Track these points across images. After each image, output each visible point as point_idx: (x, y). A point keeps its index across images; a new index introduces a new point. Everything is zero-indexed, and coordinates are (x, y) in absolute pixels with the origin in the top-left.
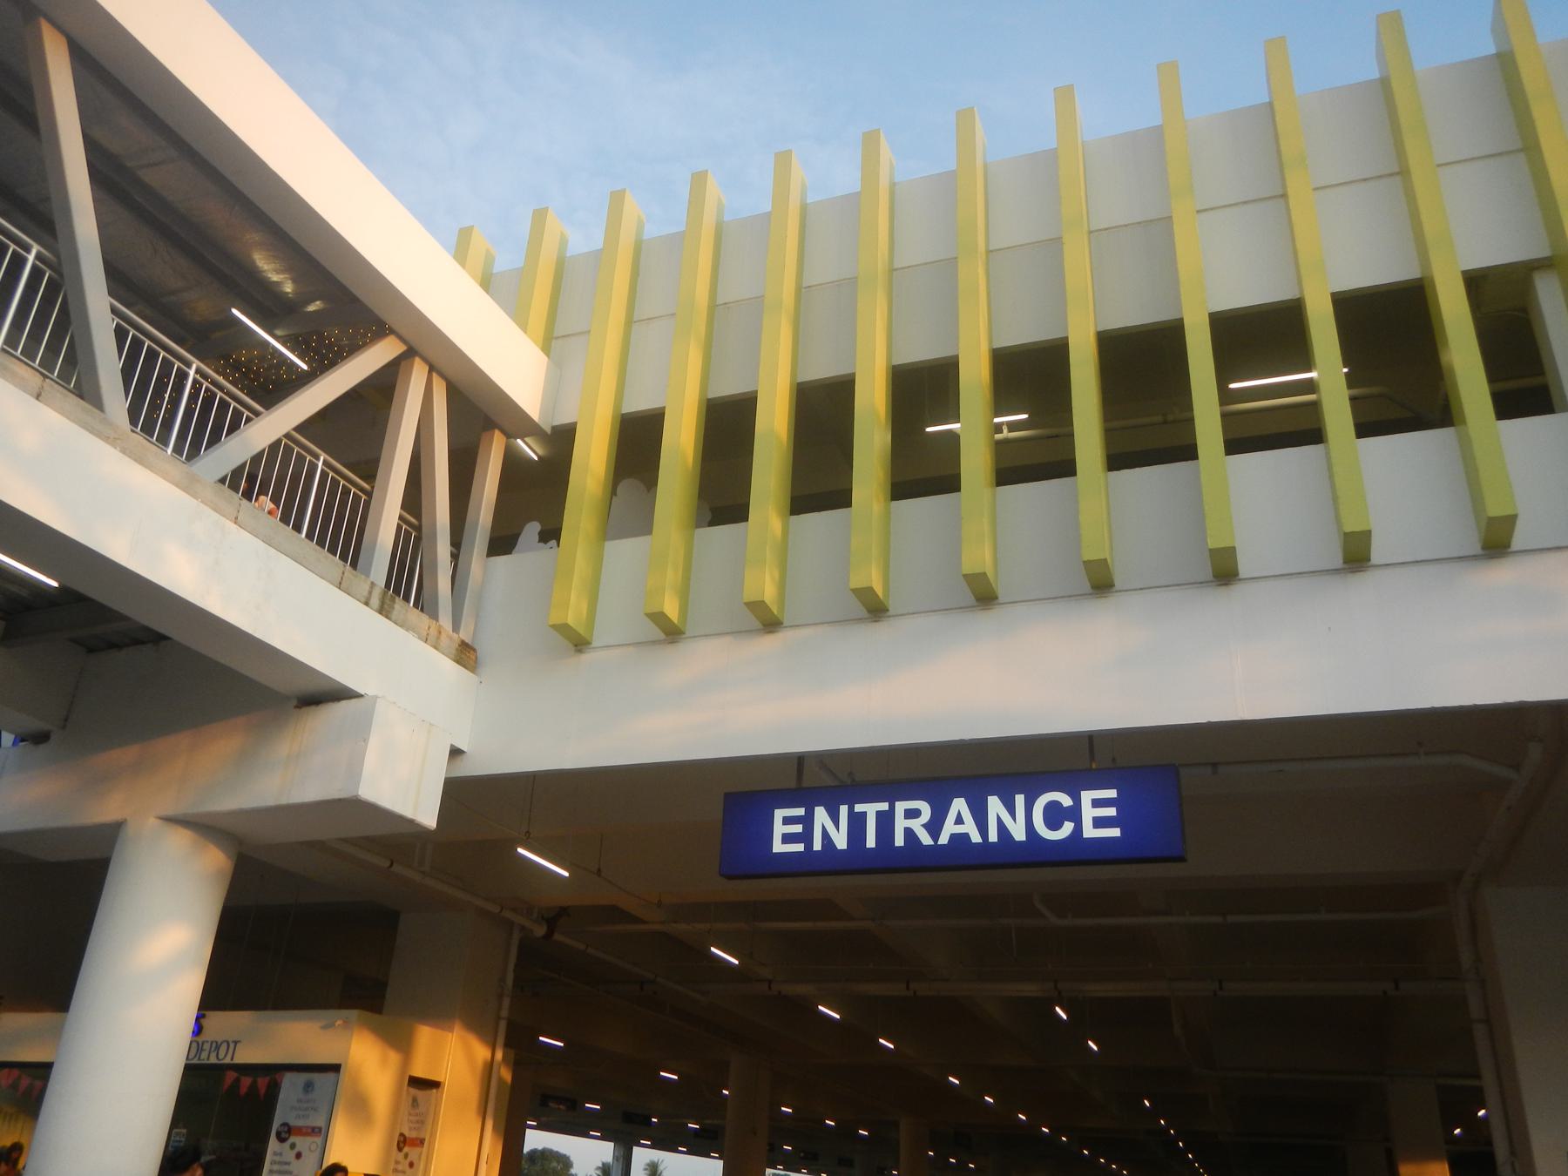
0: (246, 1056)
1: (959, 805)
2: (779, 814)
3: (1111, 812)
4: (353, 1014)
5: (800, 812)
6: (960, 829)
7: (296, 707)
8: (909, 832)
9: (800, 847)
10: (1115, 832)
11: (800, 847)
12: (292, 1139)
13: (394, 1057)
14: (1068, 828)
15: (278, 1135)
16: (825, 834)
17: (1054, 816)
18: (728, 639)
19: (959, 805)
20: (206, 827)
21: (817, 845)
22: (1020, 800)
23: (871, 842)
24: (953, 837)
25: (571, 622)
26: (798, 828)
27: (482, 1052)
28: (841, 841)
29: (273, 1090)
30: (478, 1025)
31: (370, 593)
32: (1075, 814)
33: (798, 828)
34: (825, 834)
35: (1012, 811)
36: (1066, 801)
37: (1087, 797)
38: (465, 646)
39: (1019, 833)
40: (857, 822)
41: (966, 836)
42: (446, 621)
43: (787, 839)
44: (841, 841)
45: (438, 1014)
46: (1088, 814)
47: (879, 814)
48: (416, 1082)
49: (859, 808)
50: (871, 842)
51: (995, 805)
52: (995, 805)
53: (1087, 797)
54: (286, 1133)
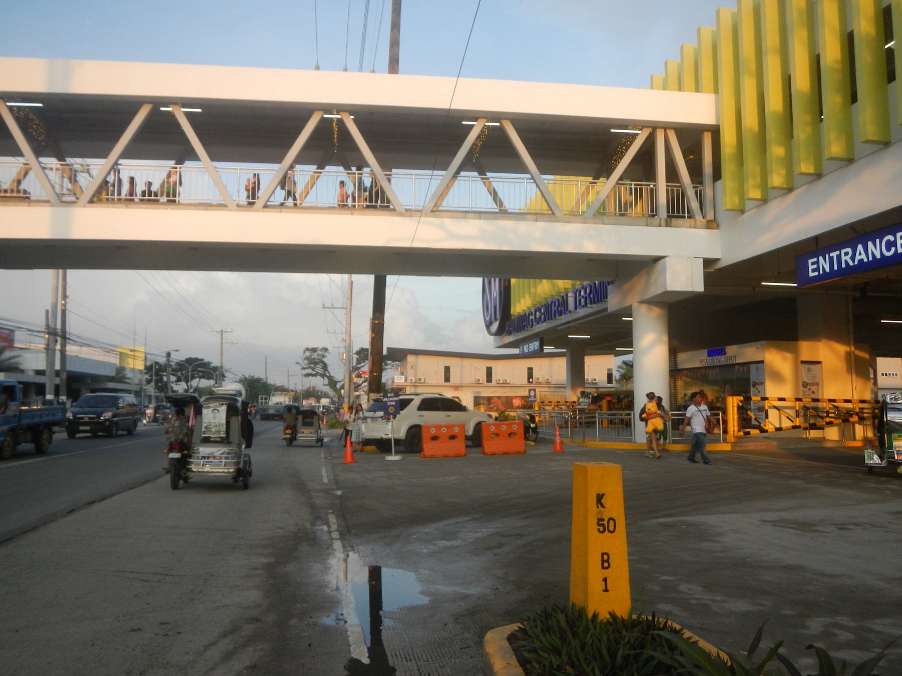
0: (739, 361)
1: (860, 247)
2: (810, 261)
4: (764, 342)
5: (815, 260)
6: (860, 257)
7: (653, 264)
8: (846, 262)
9: (816, 274)
11: (816, 274)
12: (757, 387)
13: (789, 356)
14: (893, 249)
15: (753, 385)
17: (890, 245)
18: (779, 199)
19: (860, 247)
20: (652, 302)
21: (821, 272)
22: (878, 241)
23: (836, 268)
25: (728, 207)
27: (842, 349)
28: (828, 270)
29: (749, 369)
30: (835, 335)
31: (660, 222)
33: (815, 266)
36: (891, 238)
38: (709, 221)
39: (878, 256)
40: (831, 259)
41: (862, 260)
42: (699, 217)
43: (813, 271)
44: (828, 270)
45: (813, 335)
47: (837, 256)
48: (803, 362)
50: (836, 268)
51: (870, 244)
52: (870, 244)
54: (755, 384)
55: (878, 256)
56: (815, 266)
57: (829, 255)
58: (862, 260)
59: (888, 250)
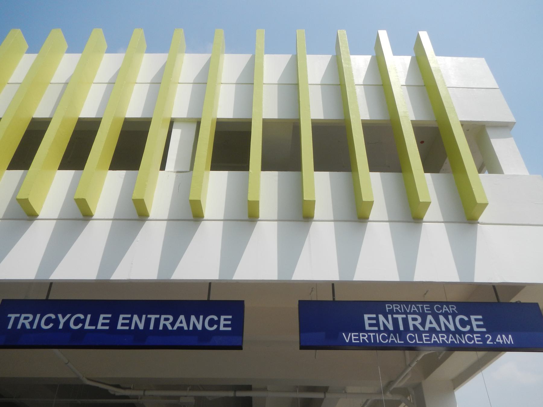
1: (182, 317)
2: (121, 316)
3: (229, 322)
5: (129, 316)
6: (181, 325)
8: (165, 325)
9: (127, 328)
10: (230, 329)
11: (127, 328)
14: (215, 327)
16: (136, 324)
19: (182, 317)
21: (133, 327)
22: (201, 317)
23: (151, 327)
24: (178, 327)
26: (128, 321)
28: (141, 326)
32: (218, 322)
33: (128, 321)
34: (136, 324)
35: (198, 321)
36: (216, 318)
37: (222, 317)
39: (199, 327)
40: (148, 321)
41: (183, 327)
43: (123, 325)
44: (141, 326)
46: (222, 322)
47: (156, 319)
49: (149, 316)
50: (151, 327)
51: (193, 318)
52: (193, 318)
53: (222, 317)
55: (199, 327)
58: (183, 327)
59: (211, 325)
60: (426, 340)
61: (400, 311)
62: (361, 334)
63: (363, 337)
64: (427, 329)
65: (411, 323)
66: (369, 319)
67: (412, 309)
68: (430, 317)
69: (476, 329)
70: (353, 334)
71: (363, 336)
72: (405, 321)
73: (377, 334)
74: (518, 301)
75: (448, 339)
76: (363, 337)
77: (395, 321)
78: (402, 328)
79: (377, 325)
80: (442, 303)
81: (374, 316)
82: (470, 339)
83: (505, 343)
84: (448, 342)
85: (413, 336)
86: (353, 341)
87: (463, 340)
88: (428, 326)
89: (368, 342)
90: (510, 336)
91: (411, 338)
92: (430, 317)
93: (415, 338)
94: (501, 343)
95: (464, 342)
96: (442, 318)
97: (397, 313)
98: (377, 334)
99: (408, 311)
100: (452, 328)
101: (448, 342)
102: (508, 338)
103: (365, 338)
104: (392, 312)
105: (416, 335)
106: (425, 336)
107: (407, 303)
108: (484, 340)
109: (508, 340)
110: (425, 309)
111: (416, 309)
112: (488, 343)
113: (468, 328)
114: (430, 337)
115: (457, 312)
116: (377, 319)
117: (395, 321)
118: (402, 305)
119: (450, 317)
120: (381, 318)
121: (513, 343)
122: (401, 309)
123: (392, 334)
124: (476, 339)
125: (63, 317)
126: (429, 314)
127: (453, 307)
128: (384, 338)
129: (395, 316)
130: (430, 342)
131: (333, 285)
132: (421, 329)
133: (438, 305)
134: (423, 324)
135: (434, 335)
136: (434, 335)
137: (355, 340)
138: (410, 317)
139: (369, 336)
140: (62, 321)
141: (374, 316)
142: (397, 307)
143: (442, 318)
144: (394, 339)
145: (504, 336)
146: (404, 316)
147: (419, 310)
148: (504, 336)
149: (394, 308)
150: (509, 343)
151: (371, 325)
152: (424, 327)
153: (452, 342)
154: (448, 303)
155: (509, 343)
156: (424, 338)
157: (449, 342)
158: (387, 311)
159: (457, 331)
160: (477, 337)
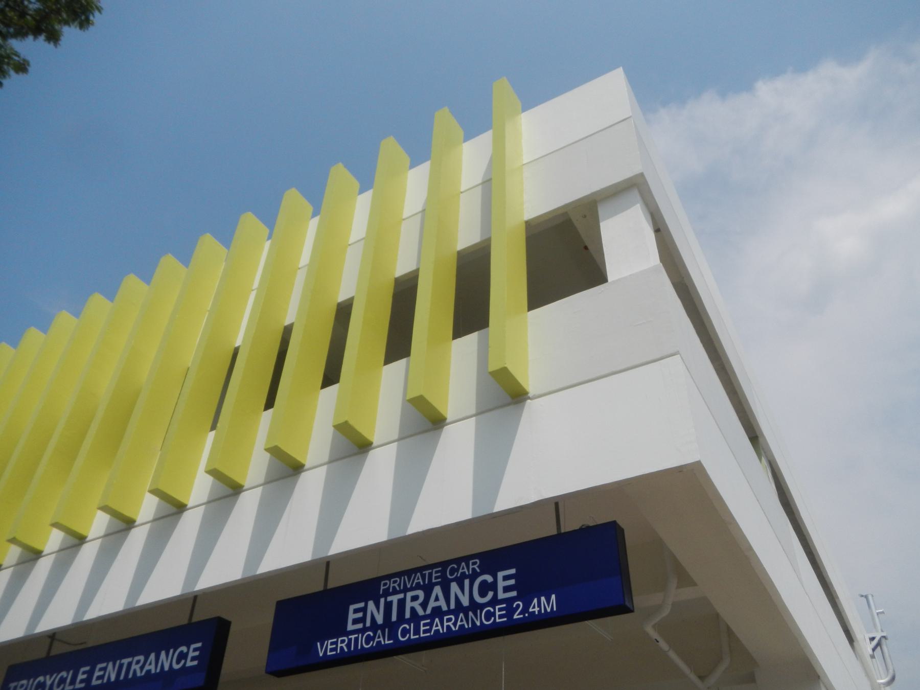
1: (152, 656)
9: (99, 682)
10: (195, 663)
19: (152, 656)
21: (105, 680)
22: (171, 651)
50: (122, 677)
52: (163, 654)
53: (193, 646)
55: (166, 668)
56: (101, 673)
57: (120, 662)
59: (178, 662)
60: (425, 632)
61: (398, 589)
62: (340, 639)
63: (342, 644)
64: (429, 611)
65: (409, 604)
66: (356, 611)
67: (416, 581)
68: (437, 590)
69: (501, 595)
70: (330, 641)
71: (343, 641)
72: (402, 603)
73: (360, 635)
74: (583, 526)
75: (455, 624)
76: (342, 644)
77: (388, 605)
78: (394, 618)
79: (362, 620)
80: (458, 561)
81: (362, 605)
82: (489, 615)
83: (543, 611)
84: (455, 627)
85: (408, 627)
86: (329, 653)
87: (477, 620)
88: (432, 604)
89: (346, 650)
90: (553, 596)
91: (405, 632)
92: (437, 590)
93: (409, 631)
94: (537, 613)
95: (478, 623)
96: (454, 587)
97: (395, 592)
98: (360, 635)
99: (409, 586)
100: (465, 602)
101: (455, 627)
102: (548, 600)
103: (343, 645)
104: (387, 593)
105: (412, 625)
106: (425, 625)
107: (409, 573)
108: (510, 611)
109: (549, 606)
110: (434, 575)
111: (420, 580)
112: (516, 617)
113: (490, 594)
114: (431, 624)
115: (478, 571)
116: (364, 610)
117: (388, 605)
118: (403, 578)
119: (467, 582)
120: (371, 605)
121: (555, 609)
122: (399, 585)
123: (379, 632)
124: (498, 613)
125: (50, 678)
126: (436, 584)
127: (474, 564)
128: (368, 641)
129: (389, 599)
130: (428, 634)
131: (328, 564)
132: (421, 612)
133: (451, 566)
134: (424, 605)
135: (437, 620)
136: (437, 620)
137: (332, 650)
138: (410, 595)
139: (350, 640)
140: (49, 683)
141: (362, 605)
142: (395, 582)
143: (454, 587)
144: (381, 639)
145: (543, 599)
146: (401, 596)
147: (424, 580)
148: (543, 599)
149: (392, 585)
150: (549, 610)
151: (355, 621)
152: (425, 608)
153: (462, 626)
154: (466, 559)
155: (549, 610)
156: (422, 628)
157: (457, 629)
158: (381, 593)
159: (475, 607)
160: (500, 610)
